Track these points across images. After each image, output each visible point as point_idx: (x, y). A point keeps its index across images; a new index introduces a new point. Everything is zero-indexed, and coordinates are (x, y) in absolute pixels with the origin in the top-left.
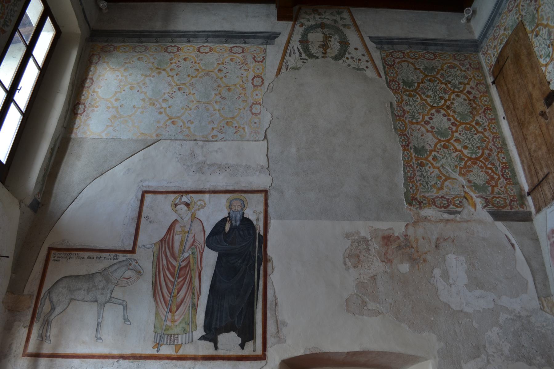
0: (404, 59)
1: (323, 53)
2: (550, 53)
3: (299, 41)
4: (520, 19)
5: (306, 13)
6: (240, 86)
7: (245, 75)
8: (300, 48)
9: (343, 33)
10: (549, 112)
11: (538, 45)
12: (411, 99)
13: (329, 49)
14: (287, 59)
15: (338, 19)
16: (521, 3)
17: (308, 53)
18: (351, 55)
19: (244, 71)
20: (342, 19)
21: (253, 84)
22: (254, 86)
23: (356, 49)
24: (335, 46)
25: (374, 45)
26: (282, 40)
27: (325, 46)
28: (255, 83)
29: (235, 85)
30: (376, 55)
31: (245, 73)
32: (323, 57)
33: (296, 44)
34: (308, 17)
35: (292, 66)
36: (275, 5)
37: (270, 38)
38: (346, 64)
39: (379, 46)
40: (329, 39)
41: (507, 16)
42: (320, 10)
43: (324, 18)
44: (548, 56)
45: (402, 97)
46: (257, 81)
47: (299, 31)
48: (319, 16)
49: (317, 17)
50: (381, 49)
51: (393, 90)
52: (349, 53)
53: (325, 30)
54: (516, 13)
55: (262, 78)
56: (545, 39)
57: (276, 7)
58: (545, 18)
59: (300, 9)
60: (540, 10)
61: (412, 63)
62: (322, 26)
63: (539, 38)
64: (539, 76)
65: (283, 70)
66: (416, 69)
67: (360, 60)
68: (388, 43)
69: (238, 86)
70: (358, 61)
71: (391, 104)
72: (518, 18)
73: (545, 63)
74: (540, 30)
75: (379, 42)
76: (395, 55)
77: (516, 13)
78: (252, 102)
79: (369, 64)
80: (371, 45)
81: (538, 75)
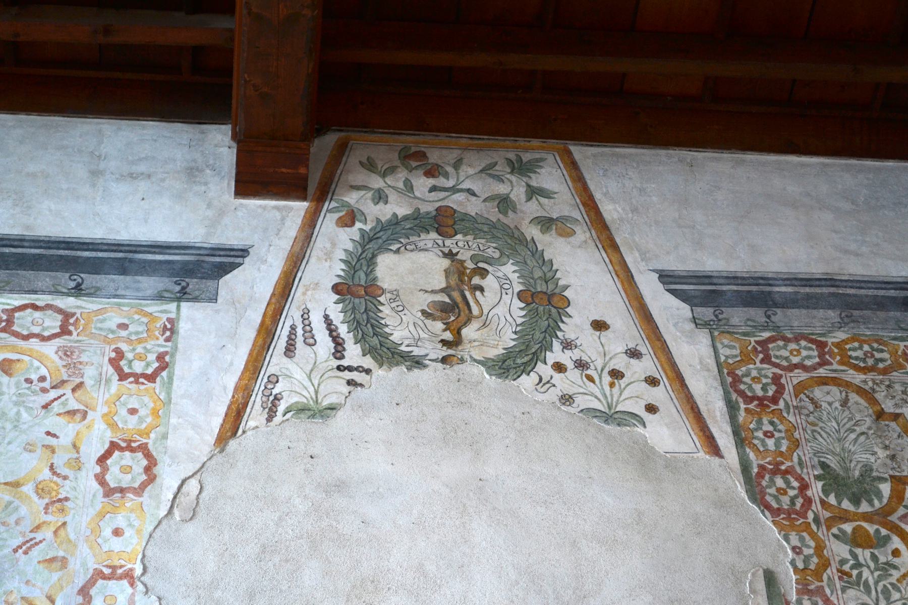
0: (822, 372)
1: (444, 342)
3: (336, 289)
5: (370, 166)
6: (40, 491)
7: (65, 439)
8: (337, 317)
9: (537, 254)
12: (864, 555)
13: (475, 325)
14: (272, 370)
15: (518, 193)
17: (375, 341)
18: (576, 354)
19: (62, 420)
20: (533, 192)
21: (101, 480)
22: (109, 492)
23: (599, 326)
24: (500, 308)
25: (684, 310)
26: (253, 283)
27: (453, 311)
28: (114, 477)
29: (16, 485)
30: (694, 352)
31: (67, 431)
32: (444, 360)
33: (316, 296)
34: (377, 182)
35: (295, 399)
36: (227, 129)
37: (198, 270)
38: (553, 395)
39: (707, 313)
40: (476, 280)
42: (434, 156)
43: (454, 190)
45: (820, 549)
46: (125, 469)
47: (335, 242)
48: (431, 182)
49: (422, 184)
50: (714, 327)
51: (775, 512)
52: (568, 345)
53: (458, 243)
55: (148, 455)
57: (234, 137)
59: (342, 149)
61: (860, 391)
62: (444, 222)
65: (255, 417)
66: (880, 415)
67: (616, 374)
68: (749, 300)
69: (28, 489)
70: (607, 379)
71: (770, 578)
75: (706, 294)
76: (779, 351)
78: (92, 565)
79: (660, 395)
80: (667, 309)
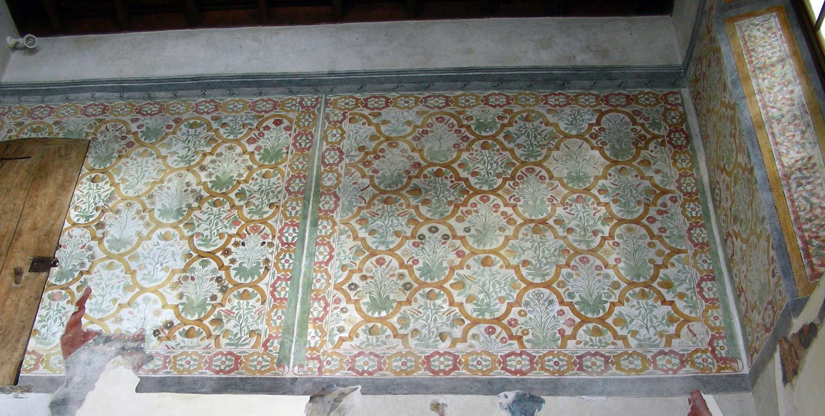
2: (92, 216)
4: (90, 138)
10: (27, 278)
11: (85, 191)
16: (108, 125)
41: (76, 113)
44: (87, 218)
54: (90, 127)
56: (99, 195)
58: (122, 174)
60: (123, 160)
63: (94, 185)
64: (53, 225)
72: (87, 134)
73: (75, 220)
74: (103, 180)
77: (90, 127)
81: (52, 222)
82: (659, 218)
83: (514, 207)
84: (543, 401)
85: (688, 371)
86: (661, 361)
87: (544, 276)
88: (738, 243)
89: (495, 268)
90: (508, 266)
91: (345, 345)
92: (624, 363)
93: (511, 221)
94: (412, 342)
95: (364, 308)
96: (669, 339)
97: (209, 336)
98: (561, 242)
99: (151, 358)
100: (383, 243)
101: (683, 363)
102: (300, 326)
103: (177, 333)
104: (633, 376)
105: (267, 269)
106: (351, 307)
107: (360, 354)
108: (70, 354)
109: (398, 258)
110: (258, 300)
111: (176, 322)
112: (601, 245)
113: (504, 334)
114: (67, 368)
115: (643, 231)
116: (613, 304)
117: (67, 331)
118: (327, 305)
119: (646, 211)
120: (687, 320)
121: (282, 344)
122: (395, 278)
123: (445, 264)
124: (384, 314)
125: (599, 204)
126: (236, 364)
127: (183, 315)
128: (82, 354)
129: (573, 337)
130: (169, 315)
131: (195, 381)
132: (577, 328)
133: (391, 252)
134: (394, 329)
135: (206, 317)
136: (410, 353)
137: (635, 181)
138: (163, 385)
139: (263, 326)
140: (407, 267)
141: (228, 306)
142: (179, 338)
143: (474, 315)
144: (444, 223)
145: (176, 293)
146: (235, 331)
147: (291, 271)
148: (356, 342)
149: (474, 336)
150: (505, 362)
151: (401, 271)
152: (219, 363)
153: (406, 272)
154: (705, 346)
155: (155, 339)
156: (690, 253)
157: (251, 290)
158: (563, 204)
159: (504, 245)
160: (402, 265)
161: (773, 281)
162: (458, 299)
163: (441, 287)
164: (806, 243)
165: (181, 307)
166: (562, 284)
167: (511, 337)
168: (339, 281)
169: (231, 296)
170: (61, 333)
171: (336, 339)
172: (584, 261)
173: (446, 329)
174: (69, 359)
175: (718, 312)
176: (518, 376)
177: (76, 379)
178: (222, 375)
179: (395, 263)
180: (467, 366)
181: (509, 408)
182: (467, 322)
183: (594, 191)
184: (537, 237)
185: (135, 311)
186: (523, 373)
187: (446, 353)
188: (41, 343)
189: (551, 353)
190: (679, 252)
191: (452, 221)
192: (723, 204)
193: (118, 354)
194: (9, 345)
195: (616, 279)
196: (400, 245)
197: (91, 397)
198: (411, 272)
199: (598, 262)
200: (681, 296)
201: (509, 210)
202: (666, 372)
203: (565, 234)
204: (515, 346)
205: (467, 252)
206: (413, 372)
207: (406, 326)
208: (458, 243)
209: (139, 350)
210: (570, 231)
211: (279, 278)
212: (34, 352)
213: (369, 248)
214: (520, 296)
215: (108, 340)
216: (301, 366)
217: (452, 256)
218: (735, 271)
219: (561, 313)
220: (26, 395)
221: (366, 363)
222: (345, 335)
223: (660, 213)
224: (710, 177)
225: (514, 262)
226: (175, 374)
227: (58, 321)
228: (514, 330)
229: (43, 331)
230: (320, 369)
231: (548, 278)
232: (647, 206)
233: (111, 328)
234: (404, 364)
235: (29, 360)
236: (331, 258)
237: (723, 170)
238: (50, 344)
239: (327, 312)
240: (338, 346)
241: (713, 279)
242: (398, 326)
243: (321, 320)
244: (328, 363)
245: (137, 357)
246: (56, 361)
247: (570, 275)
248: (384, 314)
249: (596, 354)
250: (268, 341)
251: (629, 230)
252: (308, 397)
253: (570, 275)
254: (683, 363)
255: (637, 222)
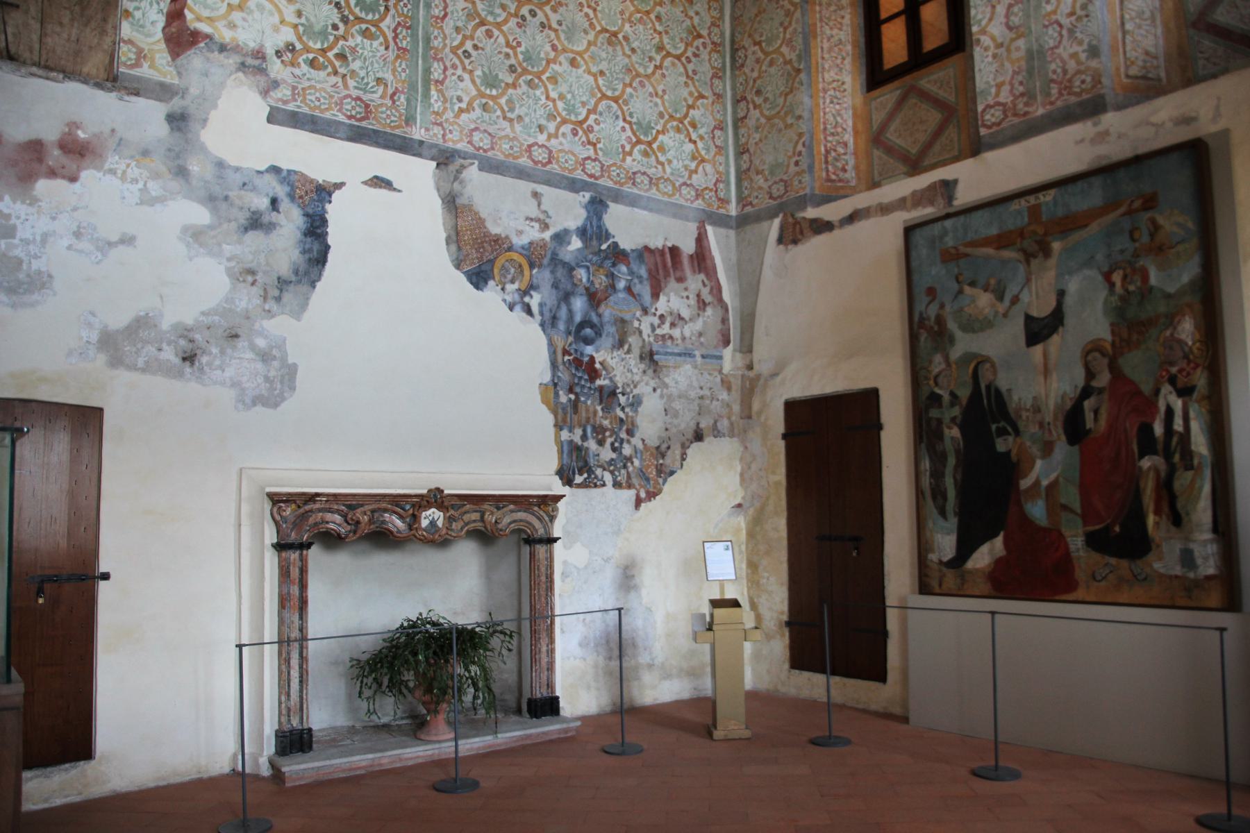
82: (693, 59)
83: (595, 10)
84: (607, 206)
85: (699, 204)
86: (685, 190)
87: (615, 90)
88: (755, 114)
89: (580, 71)
90: (589, 73)
91: (464, 116)
92: (661, 186)
93: (592, 25)
94: (518, 128)
95: (478, 81)
96: (693, 172)
97: (336, 73)
98: (627, 60)
99: (276, 84)
100: (492, 13)
101: (697, 196)
102: (423, 86)
103: (300, 60)
104: (666, 199)
105: (387, 9)
106: (466, 76)
107: (476, 129)
108: (178, 55)
109: (505, 36)
110: (381, 44)
111: (299, 46)
112: (653, 73)
113: (584, 139)
114: (179, 73)
115: (682, 70)
116: (658, 132)
117: (168, 24)
118: (445, 69)
119: (686, 50)
120: (703, 161)
121: (408, 100)
122: (502, 56)
123: (542, 55)
124: (494, 92)
125: (655, 30)
126: (367, 112)
127: (304, 38)
128: (195, 59)
129: (630, 154)
130: (288, 35)
131: (330, 123)
132: (634, 146)
133: (498, 26)
134: (503, 111)
135: (331, 48)
136: (515, 138)
137: (681, 16)
138: (295, 120)
139: (389, 76)
140: (512, 48)
141: (351, 43)
142: (305, 68)
143: (564, 113)
144: (541, 9)
145: (293, 8)
146: (362, 73)
147: (411, 18)
148: (473, 115)
149: (564, 134)
150: (583, 165)
151: (509, 50)
152: (349, 107)
153: (510, 52)
154: (712, 186)
155: (279, 61)
156: (711, 100)
157: (373, 29)
158: (630, 22)
159: (587, 50)
160: (508, 45)
161: (793, 169)
162: (553, 95)
163: (540, 79)
164: (827, 152)
165: (301, 29)
166: (626, 103)
167: (589, 143)
168: (455, 43)
169: (353, 30)
170: (161, 24)
171: (456, 108)
172: (642, 84)
173: (543, 122)
174: (180, 61)
175: (721, 159)
176: (592, 180)
177: (194, 91)
178: (353, 122)
179: (502, 40)
180: (558, 162)
181: (586, 207)
182: (559, 119)
183: (653, 16)
184: (610, 49)
185: (250, 18)
186: (596, 179)
187: (543, 146)
188: (138, 31)
189: (614, 164)
190: (702, 97)
191: (547, 9)
192: (746, 70)
193: (238, 70)
194: (93, 24)
195: (662, 109)
196: (506, 21)
197: (213, 115)
198: (516, 54)
199: (651, 90)
200: (701, 138)
201: (590, 12)
202: (687, 200)
203: (629, 53)
204: (591, 153)
205: (560, 48)
206: (518, 158)
207: (512, 110)
208: (553, 35)
209: (261, 71)
210: (633, 50)
211: (399, 24)
212: (130, 42)
213: (479, 15)
214: (596, 105)
215: (223, 48)
216: (427, 130)
217: (548, 48)
218: (742, 131)
219: (623, 129)
220: (133, 98)
221: (481, 140)
222: (464, 105)
223: (696, 55)
224: (733, 35)
225: (594, 69)
226: (305, 110)
227: (155, 6)
228: (591, 136)
229: (138, 14)
230: (444, 136)
231: (617, 93)
232: (687, 45)
233: (226, 35)
234: (511, 148)
235: (126, 54)
236: (446, 15)
237: (759, 43)
238: (149, 35)
239: (446, 77)
240: (457, 116)
241: (721, 129)
242: (506, 109)
243: (442, 83)
244: (451, 132)
245: (262, 80)
246: (164, 62)
247: (631, 96)
248: (494, 92)
249: (644, 173)
250: (394, 94)
251: (673, 64)
252: (434, 164)
253: (631, 96)
254: (697, 196)
255: (678, 57)
